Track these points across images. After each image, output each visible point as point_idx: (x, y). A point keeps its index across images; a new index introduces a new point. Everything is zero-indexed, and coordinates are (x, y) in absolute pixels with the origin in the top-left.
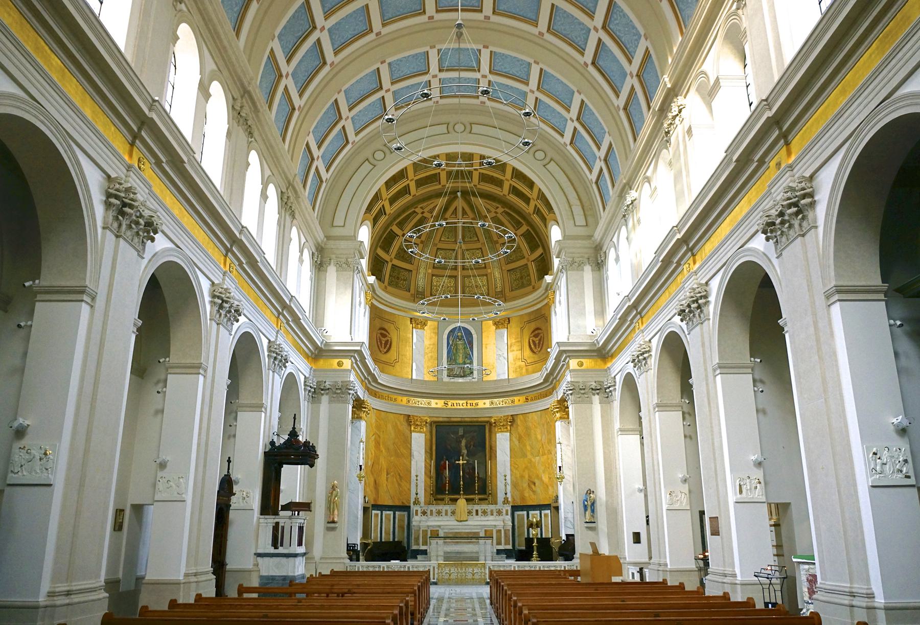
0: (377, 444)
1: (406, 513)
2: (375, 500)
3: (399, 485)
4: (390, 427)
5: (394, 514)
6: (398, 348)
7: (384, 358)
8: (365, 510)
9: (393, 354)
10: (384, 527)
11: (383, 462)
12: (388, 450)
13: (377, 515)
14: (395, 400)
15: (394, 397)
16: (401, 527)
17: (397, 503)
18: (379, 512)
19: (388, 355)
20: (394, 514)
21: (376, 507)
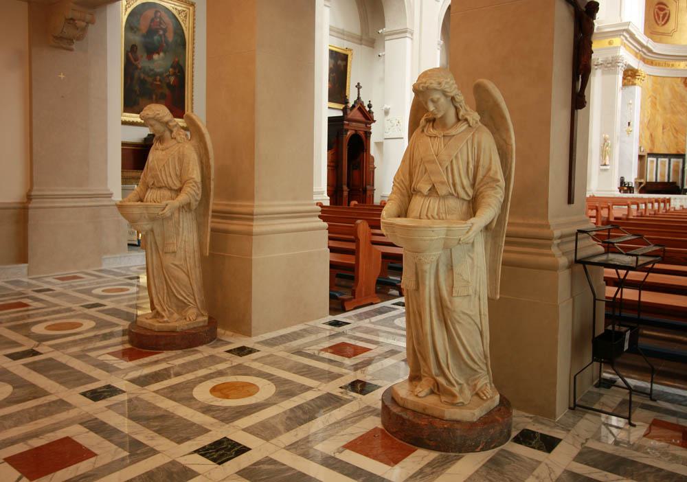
0: (654, 104)
1: (681, 160)
2: (650, 150)
3: (676, 137)
4: (667, 90)
5: (670, 161)
6: (677, 17)
7: (661, 29)
8: (641, 157)
9: (671, 25)
10: (658, 171)
11: (659, 119)
12: (665, 108)
13: (653, 161)
14: (673, 65)
15: (671, 63)
16: (676, 171)
17: (674, 152)
18: (655, 159)
19: (666, 26)
20: (670, 161)
21: (650, 155)
